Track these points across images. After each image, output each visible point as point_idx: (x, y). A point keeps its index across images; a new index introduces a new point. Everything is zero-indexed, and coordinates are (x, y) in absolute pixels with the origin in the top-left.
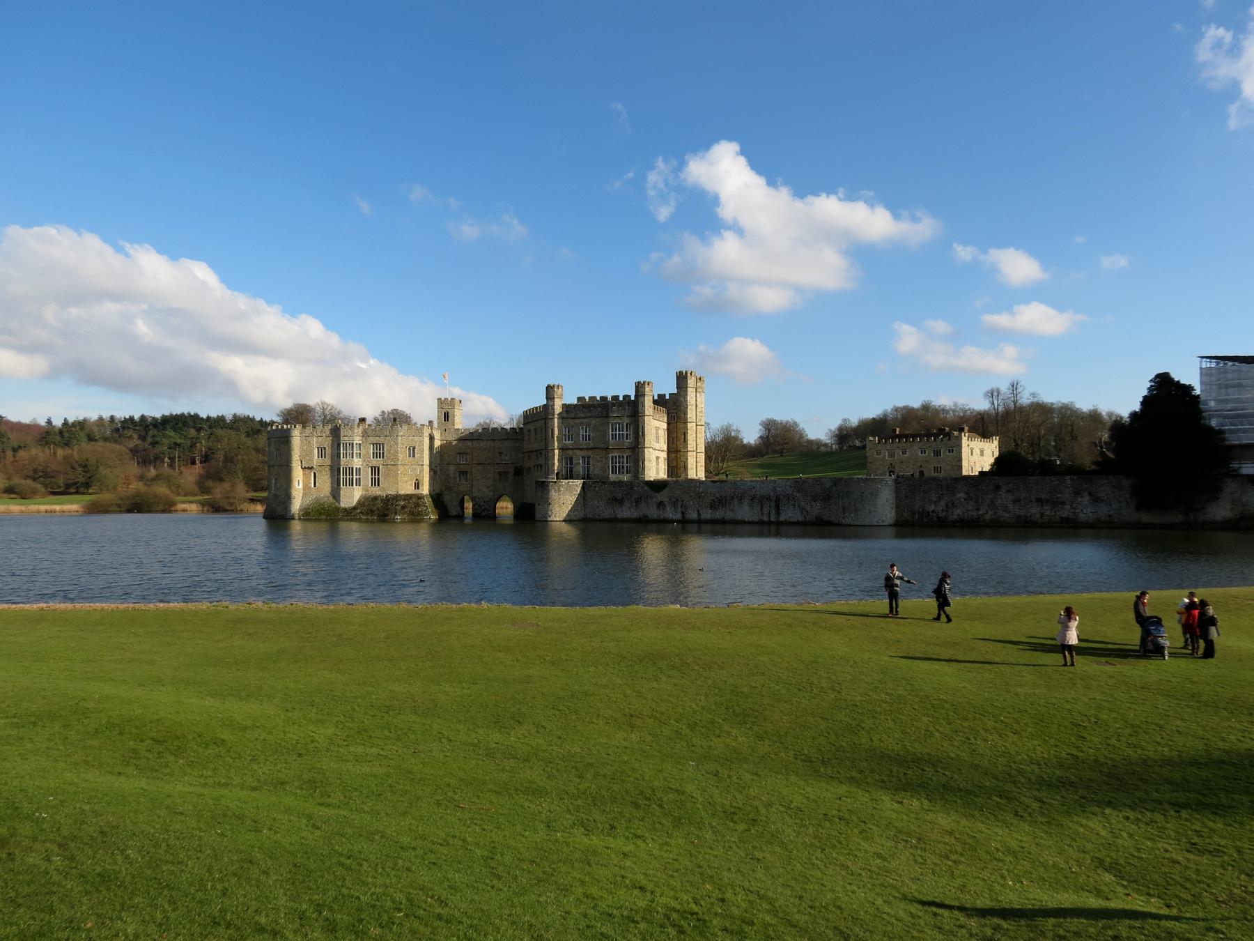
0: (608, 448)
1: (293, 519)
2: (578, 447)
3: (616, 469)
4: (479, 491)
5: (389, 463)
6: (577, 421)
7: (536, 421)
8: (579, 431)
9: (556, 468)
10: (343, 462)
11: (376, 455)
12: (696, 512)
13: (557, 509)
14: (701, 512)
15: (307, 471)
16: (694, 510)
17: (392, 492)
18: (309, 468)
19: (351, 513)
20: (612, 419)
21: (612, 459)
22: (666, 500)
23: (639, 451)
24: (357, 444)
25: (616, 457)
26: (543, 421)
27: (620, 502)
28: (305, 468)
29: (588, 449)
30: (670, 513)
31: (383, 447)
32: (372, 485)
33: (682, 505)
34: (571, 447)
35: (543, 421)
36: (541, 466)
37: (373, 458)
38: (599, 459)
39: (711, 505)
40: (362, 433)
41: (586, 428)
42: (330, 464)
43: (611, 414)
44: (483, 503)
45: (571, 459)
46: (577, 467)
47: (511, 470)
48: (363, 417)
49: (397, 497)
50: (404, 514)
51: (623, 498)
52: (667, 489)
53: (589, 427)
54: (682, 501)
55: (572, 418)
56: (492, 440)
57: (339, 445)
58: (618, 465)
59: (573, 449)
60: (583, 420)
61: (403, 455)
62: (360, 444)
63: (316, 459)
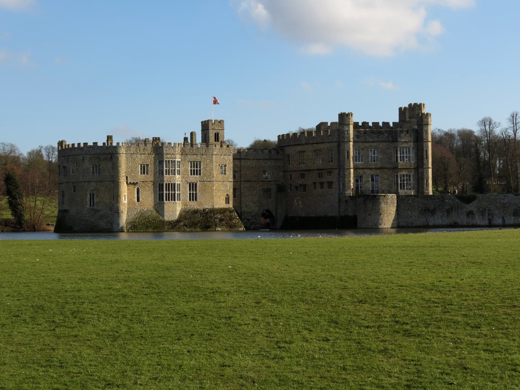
0: (396, 168)
1: (123, 231)
2: (367, 167)
3: (404, 186)
4: (247, 206)
5: (205, 179)
6: (367, 145)
7: (318, 143)
8: (369, 153)
9: (352, 185)
10: (167, 179)
11: (193, 173)
12: (501, 219)
13: (386, 218)
14: (505, 219)
15: (131, 187)
16: (499, 217)
17: (208, 206)
18: (134, 184)
19: (175, 225)
20: (400, 143)
21: (401, 178)
22: (475, 210)
23: (423, 171)
24: (177, 161)
25: (404, 176)
26: (336, 144)
27: (433, 212)
28: (130, 183)
29: (376, 169)
30: (478, 220)
31: (200, 165)
32: (190, 200)
34: (361, 167)
35: (336, 144)
36: (330, 184)
37: (191, 174)
39: (514, 213)
40: (181, 151)
41: (374, 150)
42: (152, 180)
43: (399, 140)
44: (250, 217)
45: (361, 177)
46: (367, 184)
47: (274, 188)
48: (157, 136)
49: (213, 211)
50: (223, 225)
51: (435, 209)
52: (476, 201)
53: (378, 151)
54: (489, 210)
55: (362, 142)
56: (257, 159)
57: (161, 162)
58: (405, 182)
59: (363, 169)
60: (371, 144)
61: (216, 172)
62: (179, 162)
63: (140, 177)
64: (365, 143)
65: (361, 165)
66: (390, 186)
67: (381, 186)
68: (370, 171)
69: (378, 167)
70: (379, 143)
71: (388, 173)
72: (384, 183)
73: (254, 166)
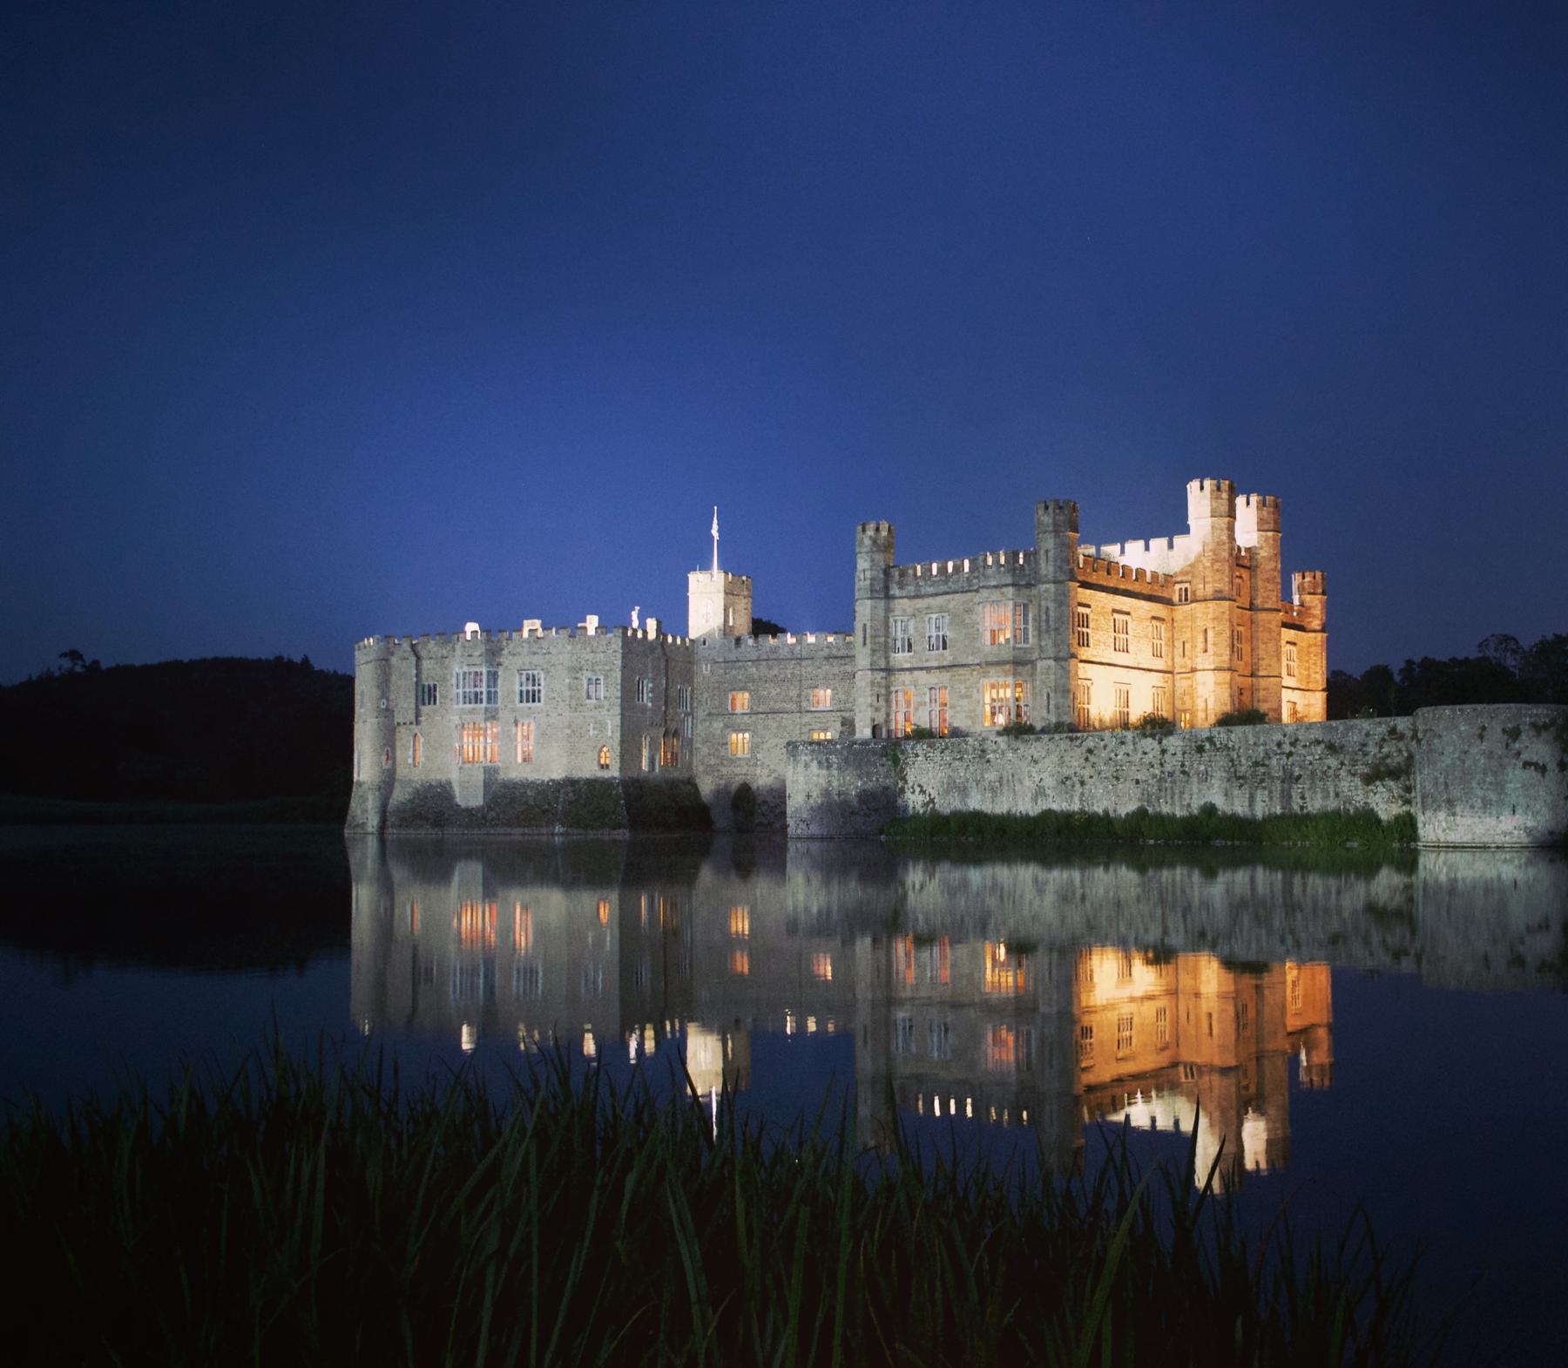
2: (920, 665)
6: (920, 603)
33: (1082, 794)
34: (907, 666)
37: (521, 702)
38: (963, 691)
46: (920, 712)
59: (911, 670)
64: (916, 601)
65: (906, 662)
66: (972, 714)
67: (952, 716)
68: (928, 676)
69: (945, 663)
70: (948, 597)
71: (969, 680)
72: (958, 708)
73: (789, 676)
